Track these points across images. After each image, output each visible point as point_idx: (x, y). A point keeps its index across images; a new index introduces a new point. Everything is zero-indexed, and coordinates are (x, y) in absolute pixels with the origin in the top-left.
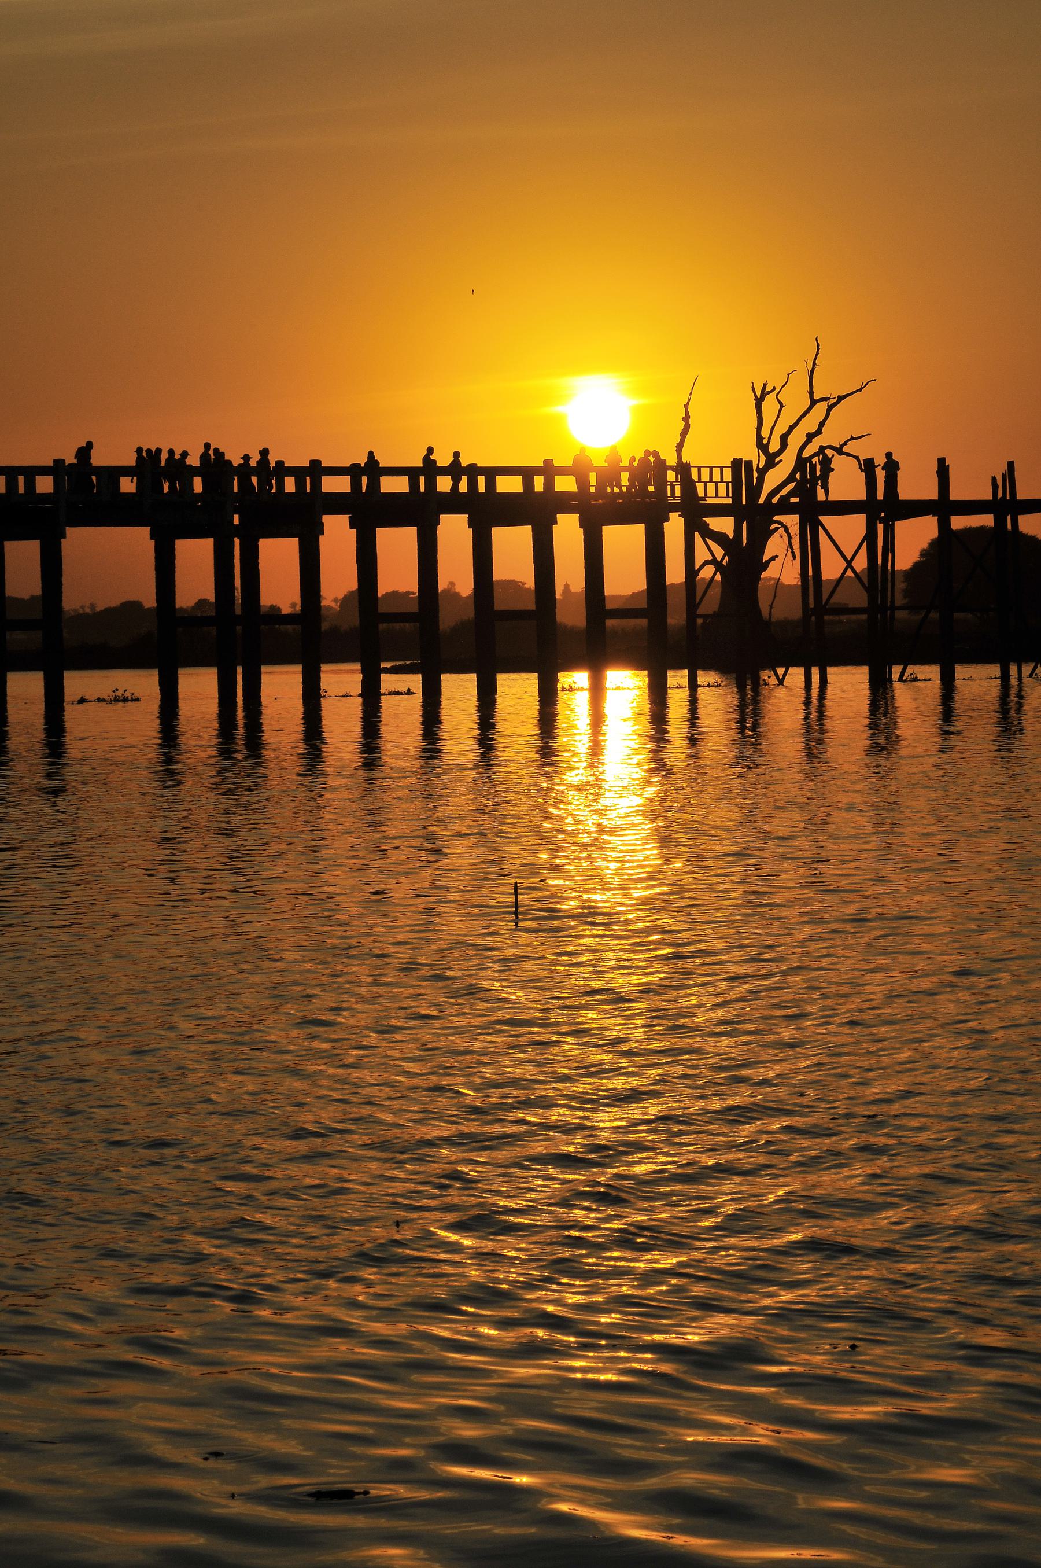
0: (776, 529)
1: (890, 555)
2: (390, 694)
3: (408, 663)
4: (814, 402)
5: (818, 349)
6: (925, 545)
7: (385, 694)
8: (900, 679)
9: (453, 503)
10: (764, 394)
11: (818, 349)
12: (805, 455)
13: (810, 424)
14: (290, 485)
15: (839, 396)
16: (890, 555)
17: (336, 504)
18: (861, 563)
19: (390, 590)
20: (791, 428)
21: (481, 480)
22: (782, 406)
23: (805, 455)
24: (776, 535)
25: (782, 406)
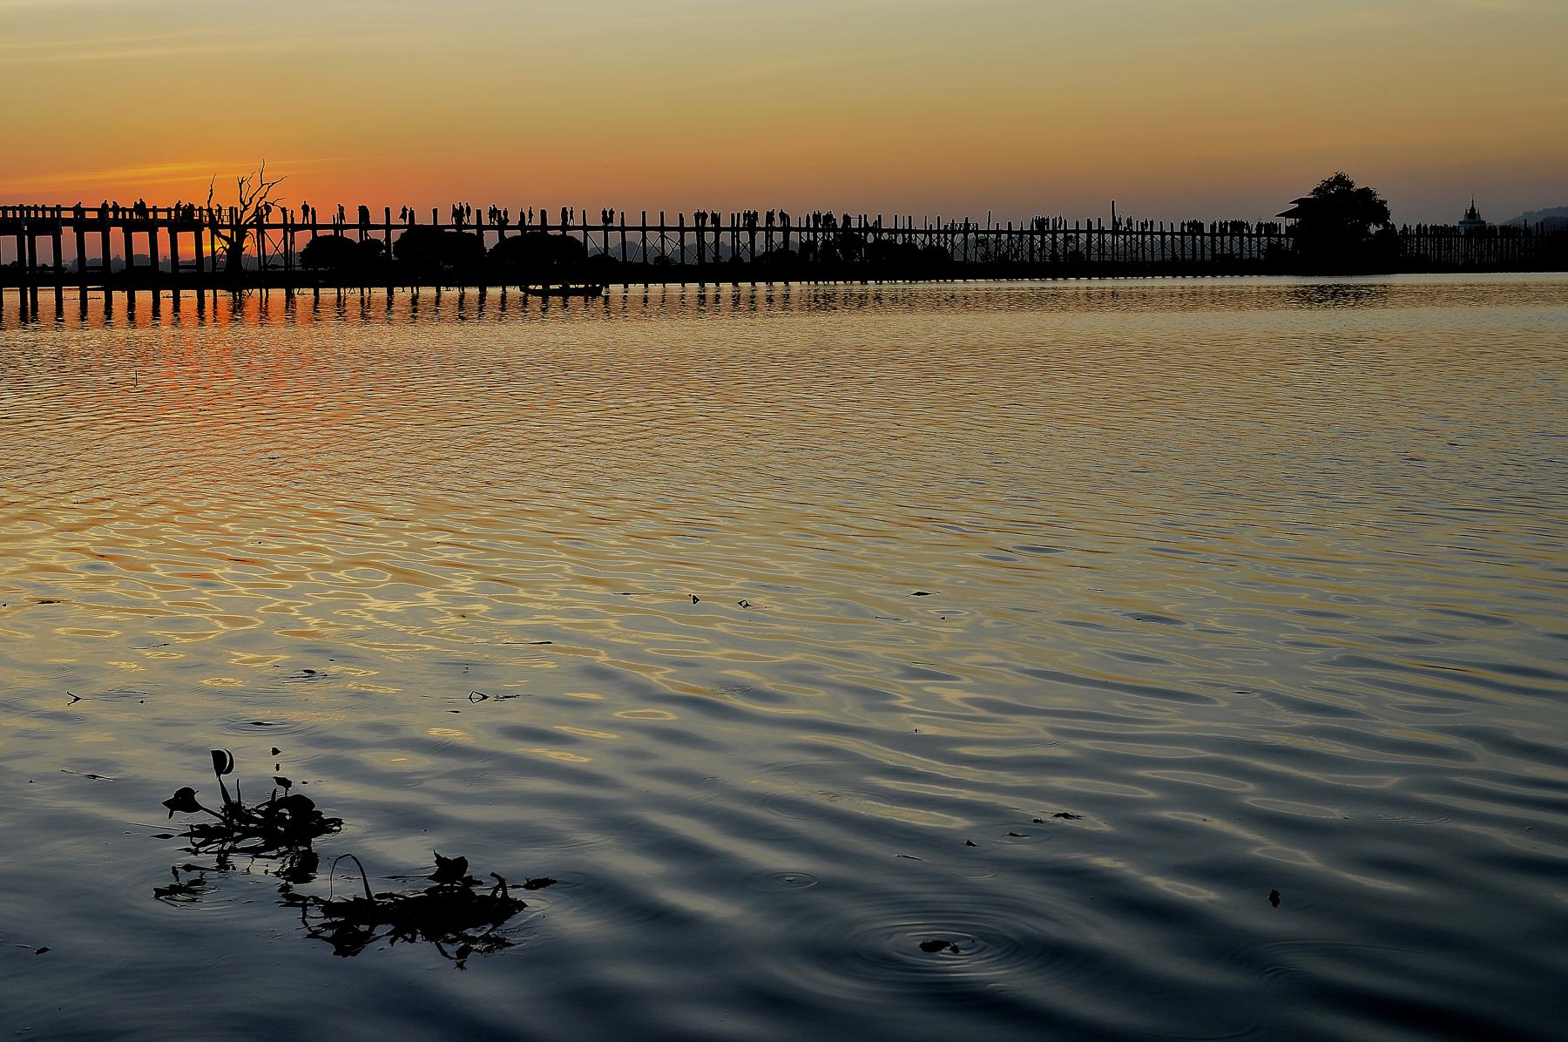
4: (263, 185)
9: (116, 222)
10: (242, 181)
14: (48, 214)
17: (67, 222)
21: (127, 213)
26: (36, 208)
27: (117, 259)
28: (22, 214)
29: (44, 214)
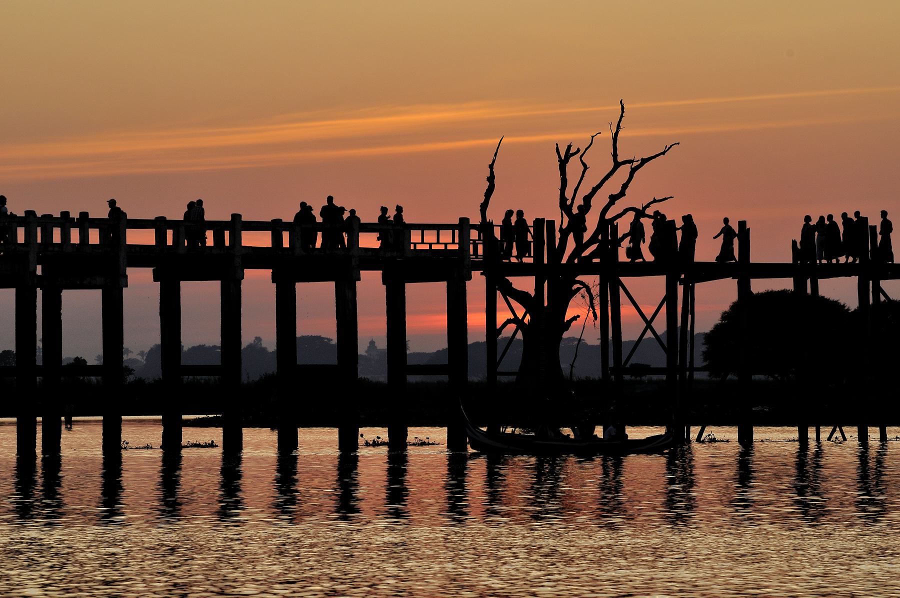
0: (578, 289)
1: (690, 316)
2: (191, 446)
3: (210, 416)
4: (617, 165)
5: (623, 112)
6: (726, 308)
7: (186, 447)
8: (699, 440)
10: (568, 155)
11: (623, 112)
12: (608, 216)
13: (613, 186)
15: (642, 159)
16: (690, 316)
18: (661, 325)
19: (196, 344)
20: (595, 190)
22: (586, 167)
23: (608, 216)
24: (578, 295)
25: (586, 167)
26: (65, 221)
27: (257, 347)
28: (30, 235)
29: (84, 236)
